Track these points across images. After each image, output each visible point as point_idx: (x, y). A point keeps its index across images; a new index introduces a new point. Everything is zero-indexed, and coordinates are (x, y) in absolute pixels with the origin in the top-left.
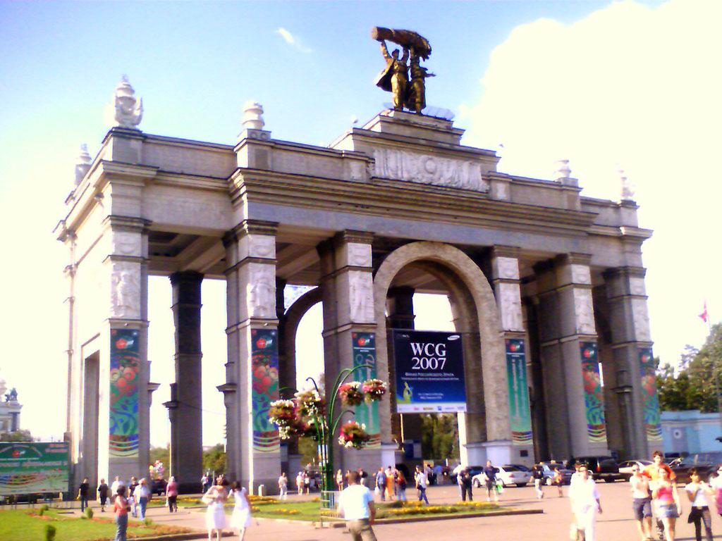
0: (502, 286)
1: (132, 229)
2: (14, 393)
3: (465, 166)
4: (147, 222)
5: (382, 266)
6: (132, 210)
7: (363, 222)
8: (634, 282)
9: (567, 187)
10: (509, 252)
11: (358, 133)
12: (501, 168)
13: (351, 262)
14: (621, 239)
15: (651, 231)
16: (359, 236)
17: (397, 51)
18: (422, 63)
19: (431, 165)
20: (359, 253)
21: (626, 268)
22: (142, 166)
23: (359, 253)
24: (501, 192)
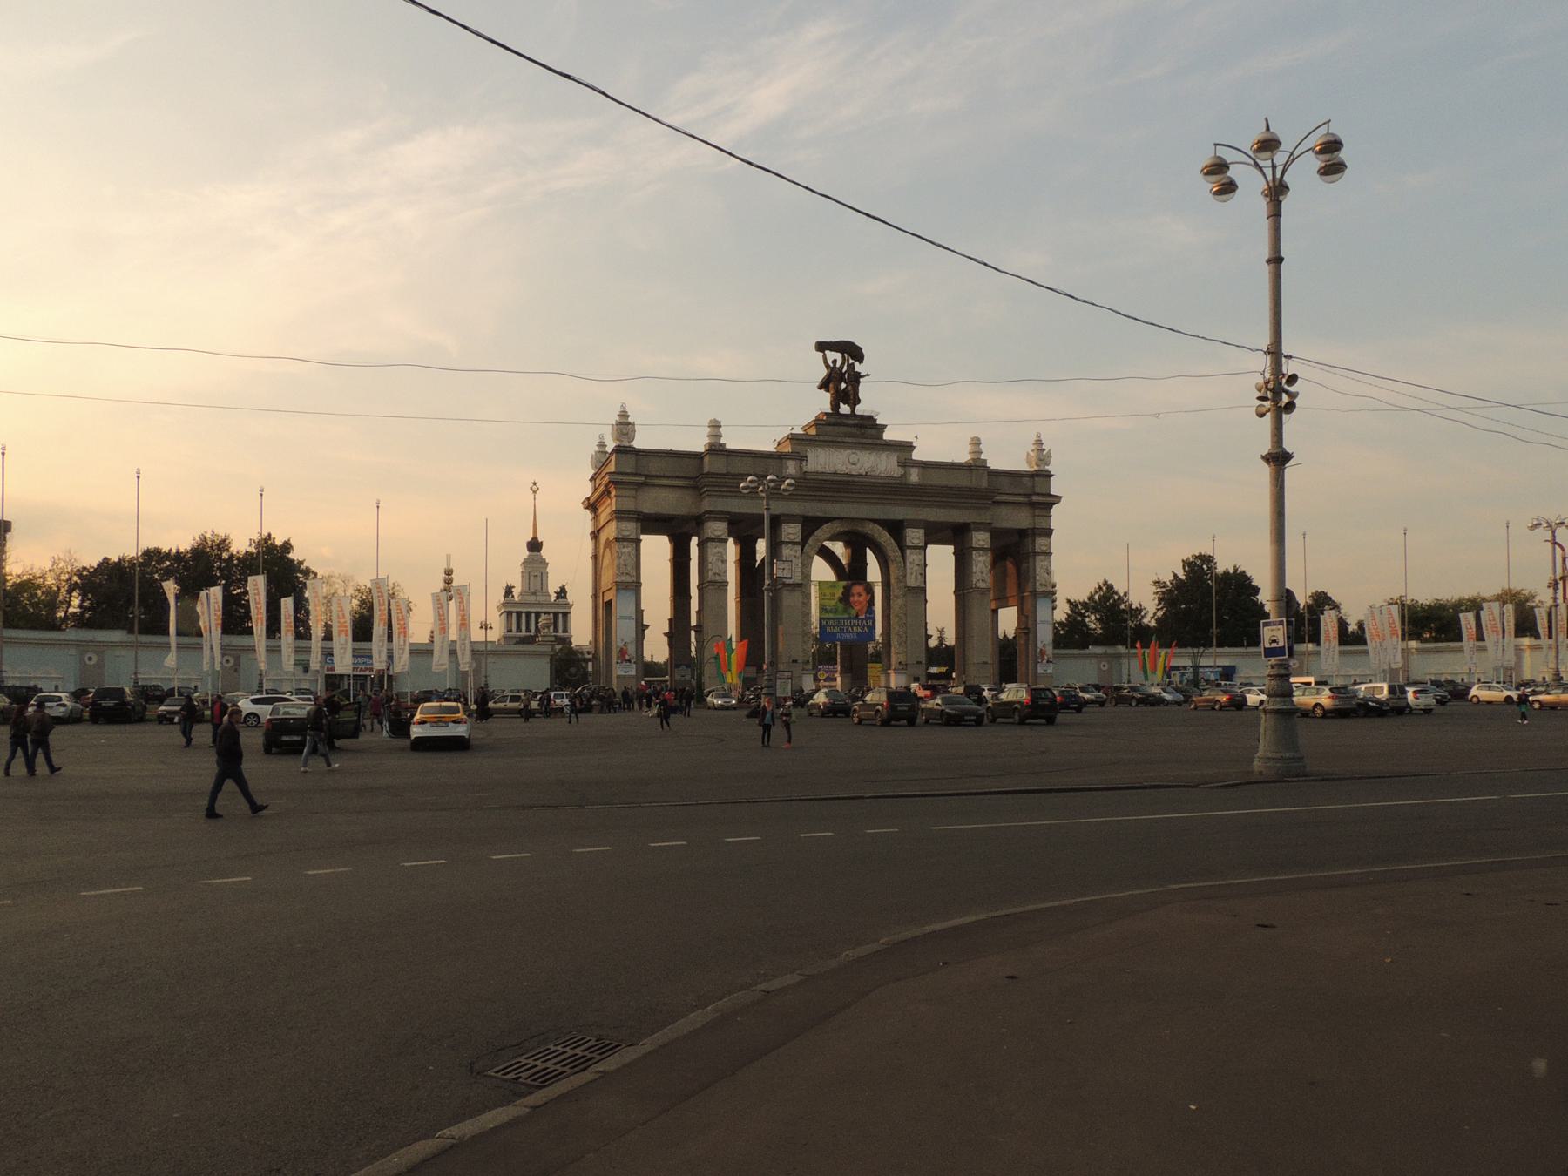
0: (908, 552)
1: (629, 519)
2: (562, 593)
3: (884, 455)
4: (639, 513)
5: (810, 541)
6: (629, 505)
7: (796, 508)
8: (1040, 542)
9: (976, 466)
10: (915, 524)
11: (793, 438)
12: (917, 455)
13: (784, 538)
14: (1033, 505)
15: (1060, 498)
16: (791, 518)
17: (835, 361)
18: (858, 367)
19: (854, 458)
20: (791, 531)
21: (1033, 529)
22: (636, 474)
23: (791, 531)
24: (914, 476)
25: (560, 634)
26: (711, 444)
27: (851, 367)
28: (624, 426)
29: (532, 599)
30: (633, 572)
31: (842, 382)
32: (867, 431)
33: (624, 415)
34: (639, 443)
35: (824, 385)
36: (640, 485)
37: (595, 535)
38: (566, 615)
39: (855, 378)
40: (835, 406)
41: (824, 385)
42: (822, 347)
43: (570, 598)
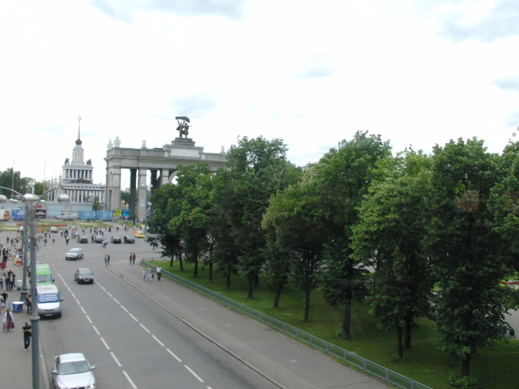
2: (89, 162)
12: (204, 151)
18: (188, 124)
24: (203, 158)
25: (88, 179)
26: (143, 147)
27: (186, 124)
28: (118, 141)
29: (76, 164)
30: (118, 183)
31: (183, 129)
32: (189, 143)
33: (117, 138)
34: (122, 146)
35: (178, 129)
36: (121, 159)
37: (107, 169)
38: (91, 171)
39: (187, 128)
40: (181, 135)
41: (178, 129)
42: (177, 118)
43: (93, 164)
